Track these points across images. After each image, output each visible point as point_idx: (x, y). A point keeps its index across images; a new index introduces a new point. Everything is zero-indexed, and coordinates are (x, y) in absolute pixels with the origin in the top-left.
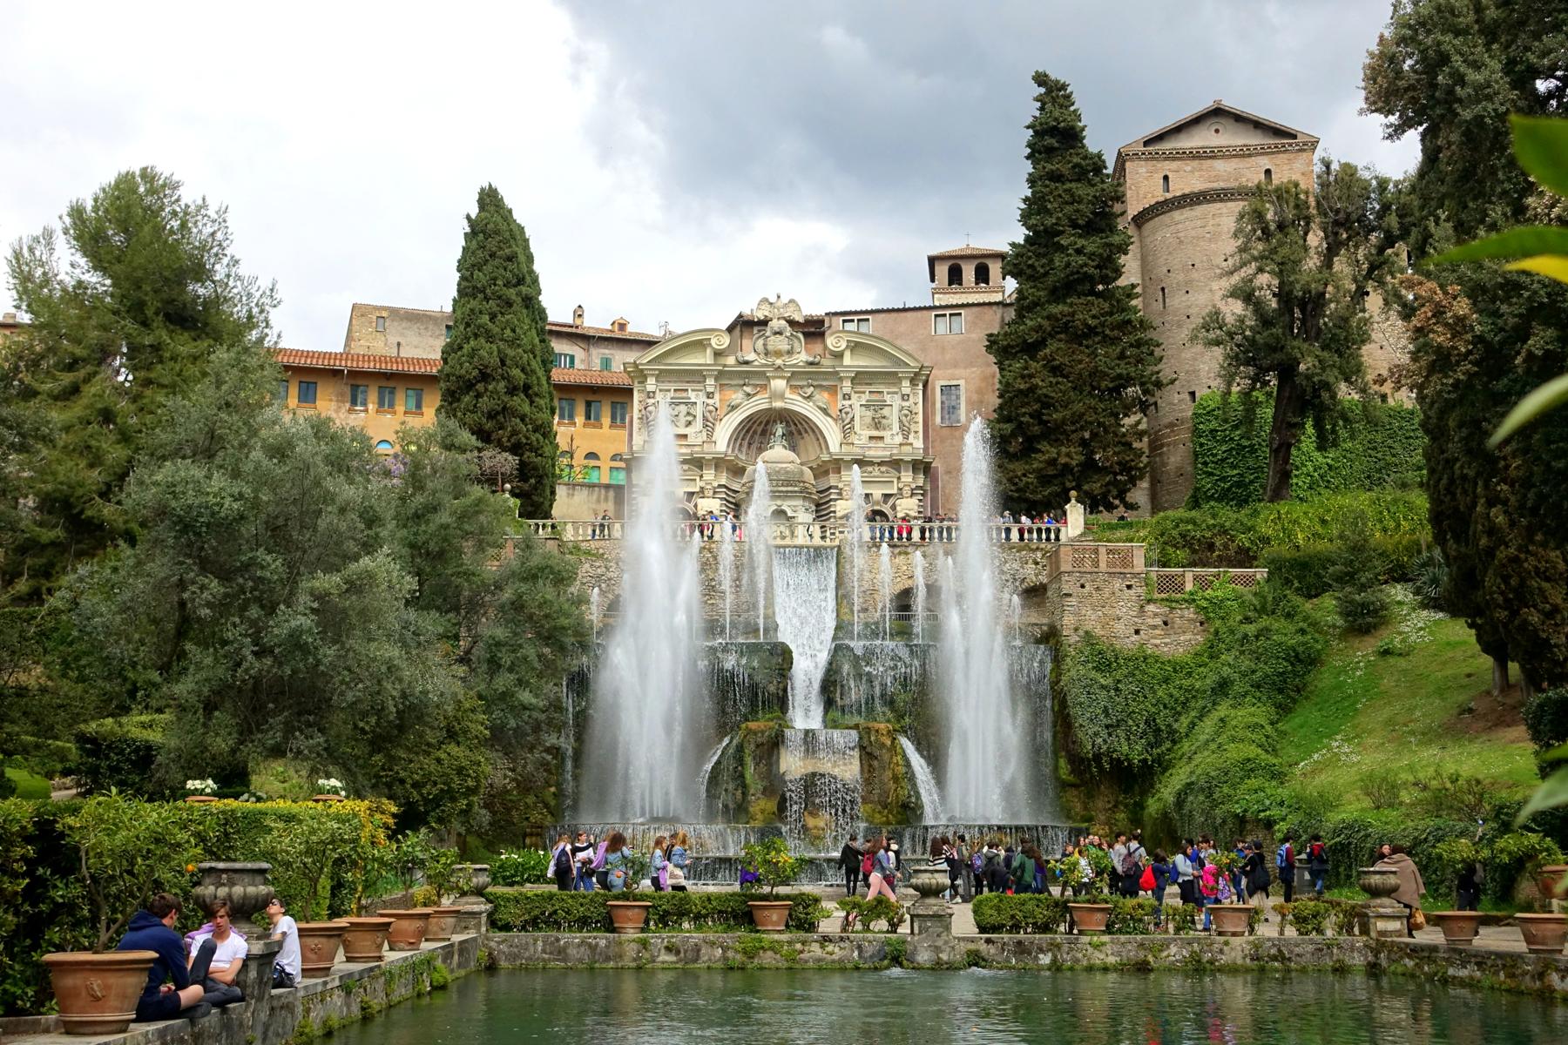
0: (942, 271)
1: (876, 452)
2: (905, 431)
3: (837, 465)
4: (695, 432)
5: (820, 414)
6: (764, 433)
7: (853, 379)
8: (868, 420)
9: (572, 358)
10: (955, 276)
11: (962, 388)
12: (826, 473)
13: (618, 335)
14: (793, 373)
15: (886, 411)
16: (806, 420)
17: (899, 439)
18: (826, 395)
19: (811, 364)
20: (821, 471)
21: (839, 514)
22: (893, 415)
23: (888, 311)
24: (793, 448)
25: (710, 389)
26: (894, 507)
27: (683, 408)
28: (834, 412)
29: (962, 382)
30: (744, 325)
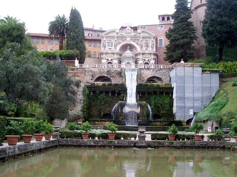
0: (161, 18)
1: (147, 52)
2: (152, 48)
3: (139, 54)
4: (113, 48)
5: (136, 44)
6: (126, 48)
7: (142, 38)
8: (145, 46)
9: (92, 35)
10: (163, 19)
11: (163, 40)
12: (137, 55)
13: (100, 30)
14: (131, 37)
15: (148, 44)
16: (134, 46)
17: (151, 49)
18: (137, 41)
19: (135, 35)
20: (136, 55)
21: (139, 63)
22: (150, 45)
23: (149, 25)
24: (131, 51)
25: (115, 40)
26: (150, 62)
27: (111, 44)
28: (139, 44)
29: (163, 39)
30: (123, 28)
